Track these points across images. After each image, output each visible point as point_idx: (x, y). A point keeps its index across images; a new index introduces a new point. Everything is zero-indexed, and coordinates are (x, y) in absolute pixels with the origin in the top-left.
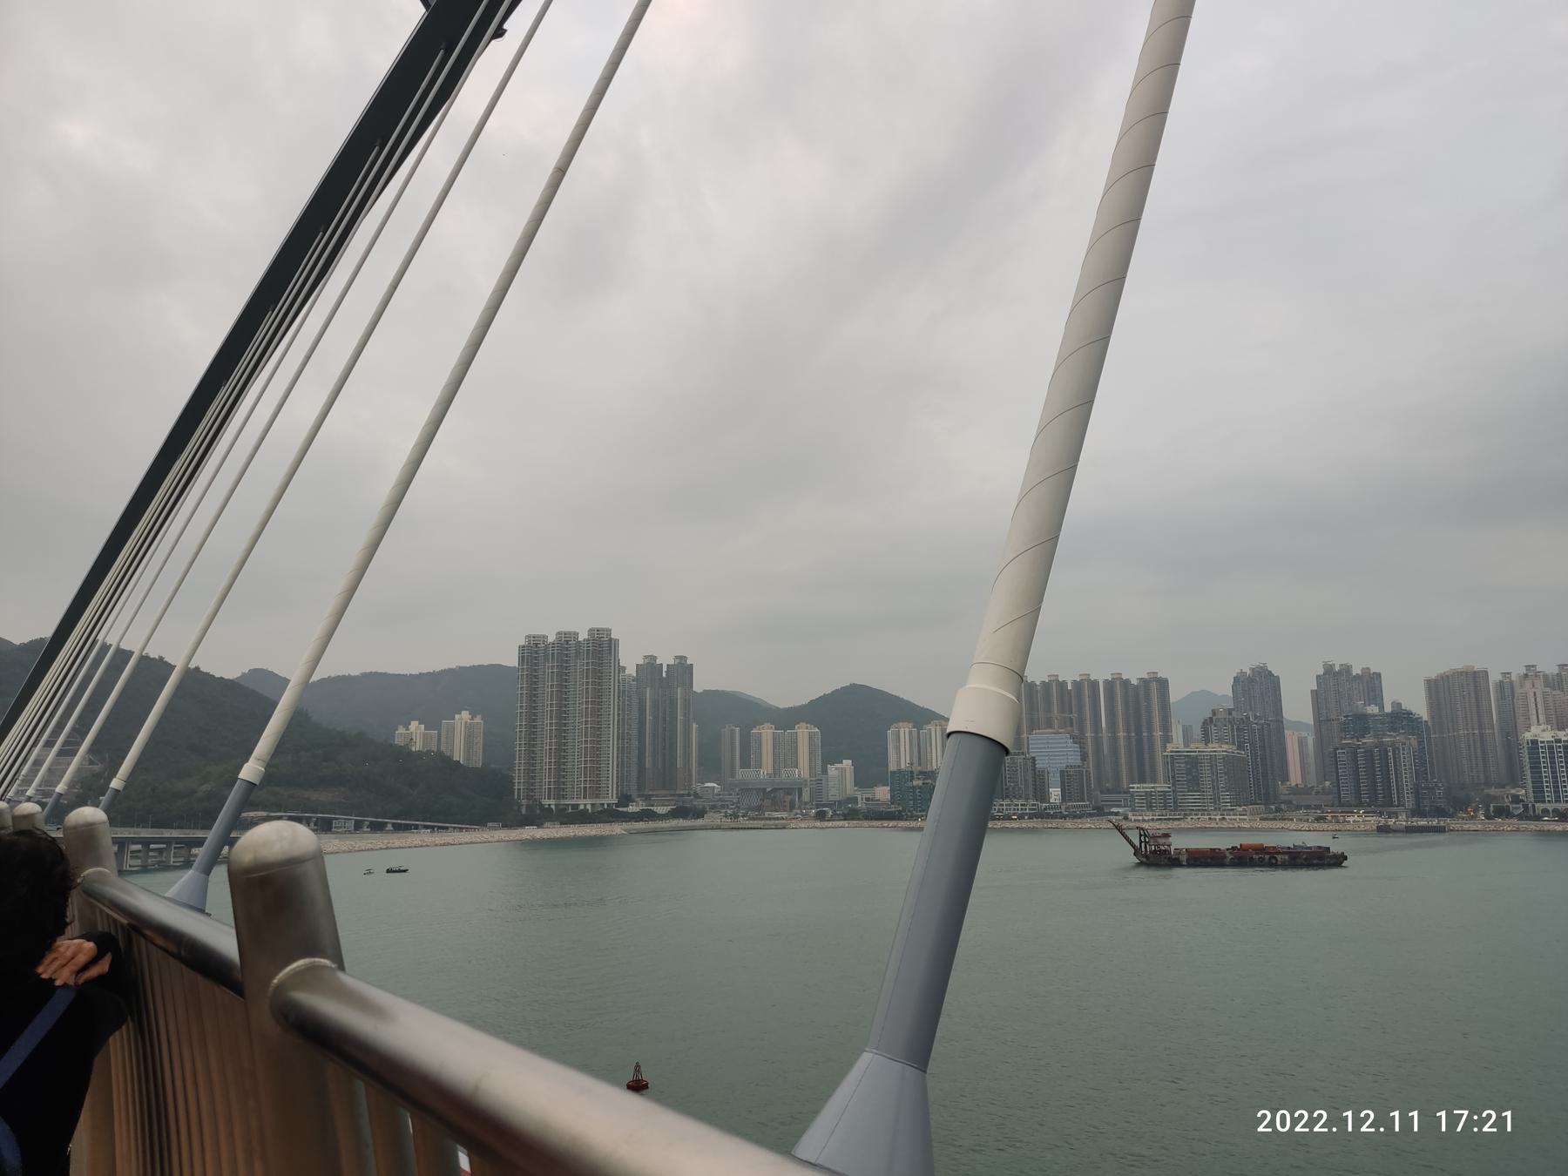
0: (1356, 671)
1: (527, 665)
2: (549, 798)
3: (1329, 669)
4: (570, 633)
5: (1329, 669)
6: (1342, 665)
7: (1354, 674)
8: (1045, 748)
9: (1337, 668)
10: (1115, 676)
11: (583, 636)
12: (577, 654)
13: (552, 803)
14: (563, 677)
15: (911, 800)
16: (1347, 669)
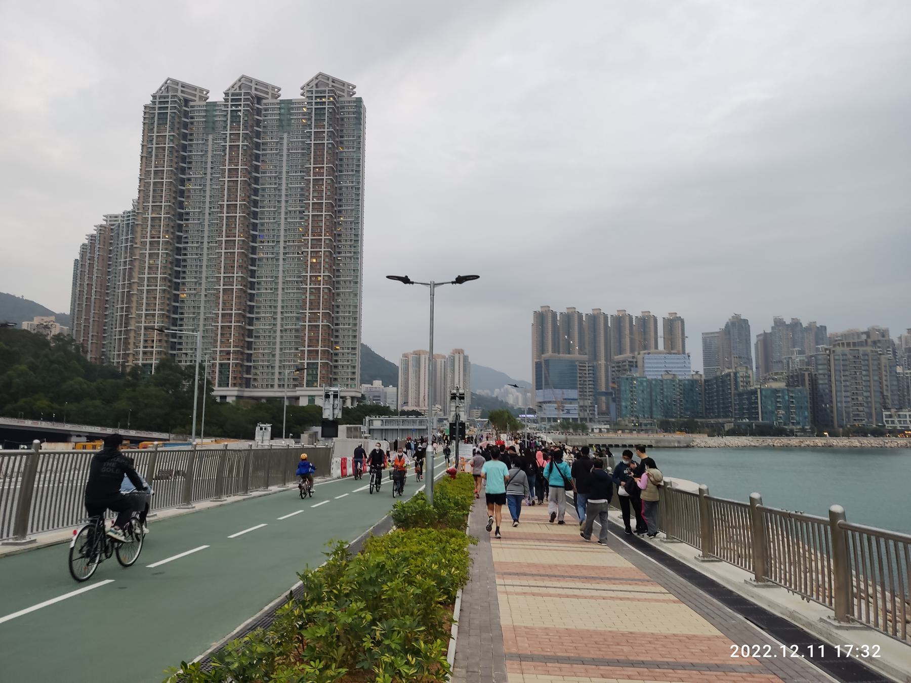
0: (805, 325)
1: (172, 129)
2: (224, 383)
3: (779, 323)
4: (266, 86)
5: (779, 323)
6: (792, 319)
7: (804, 325)
8: (661, 368)
9: (788, 322)
10: (646, 314)
11: (292, 91)
12: (283, 124)
13: (231, 393)
14: (254, 156)
15: (779, 408)
16: (796, 324)
